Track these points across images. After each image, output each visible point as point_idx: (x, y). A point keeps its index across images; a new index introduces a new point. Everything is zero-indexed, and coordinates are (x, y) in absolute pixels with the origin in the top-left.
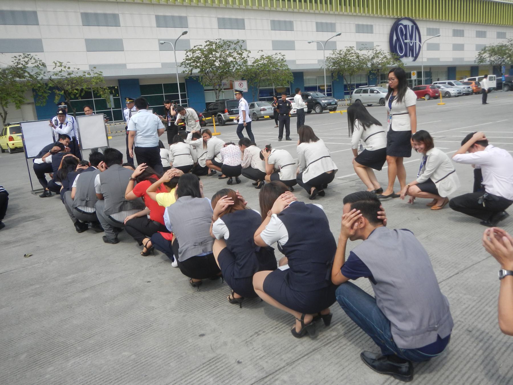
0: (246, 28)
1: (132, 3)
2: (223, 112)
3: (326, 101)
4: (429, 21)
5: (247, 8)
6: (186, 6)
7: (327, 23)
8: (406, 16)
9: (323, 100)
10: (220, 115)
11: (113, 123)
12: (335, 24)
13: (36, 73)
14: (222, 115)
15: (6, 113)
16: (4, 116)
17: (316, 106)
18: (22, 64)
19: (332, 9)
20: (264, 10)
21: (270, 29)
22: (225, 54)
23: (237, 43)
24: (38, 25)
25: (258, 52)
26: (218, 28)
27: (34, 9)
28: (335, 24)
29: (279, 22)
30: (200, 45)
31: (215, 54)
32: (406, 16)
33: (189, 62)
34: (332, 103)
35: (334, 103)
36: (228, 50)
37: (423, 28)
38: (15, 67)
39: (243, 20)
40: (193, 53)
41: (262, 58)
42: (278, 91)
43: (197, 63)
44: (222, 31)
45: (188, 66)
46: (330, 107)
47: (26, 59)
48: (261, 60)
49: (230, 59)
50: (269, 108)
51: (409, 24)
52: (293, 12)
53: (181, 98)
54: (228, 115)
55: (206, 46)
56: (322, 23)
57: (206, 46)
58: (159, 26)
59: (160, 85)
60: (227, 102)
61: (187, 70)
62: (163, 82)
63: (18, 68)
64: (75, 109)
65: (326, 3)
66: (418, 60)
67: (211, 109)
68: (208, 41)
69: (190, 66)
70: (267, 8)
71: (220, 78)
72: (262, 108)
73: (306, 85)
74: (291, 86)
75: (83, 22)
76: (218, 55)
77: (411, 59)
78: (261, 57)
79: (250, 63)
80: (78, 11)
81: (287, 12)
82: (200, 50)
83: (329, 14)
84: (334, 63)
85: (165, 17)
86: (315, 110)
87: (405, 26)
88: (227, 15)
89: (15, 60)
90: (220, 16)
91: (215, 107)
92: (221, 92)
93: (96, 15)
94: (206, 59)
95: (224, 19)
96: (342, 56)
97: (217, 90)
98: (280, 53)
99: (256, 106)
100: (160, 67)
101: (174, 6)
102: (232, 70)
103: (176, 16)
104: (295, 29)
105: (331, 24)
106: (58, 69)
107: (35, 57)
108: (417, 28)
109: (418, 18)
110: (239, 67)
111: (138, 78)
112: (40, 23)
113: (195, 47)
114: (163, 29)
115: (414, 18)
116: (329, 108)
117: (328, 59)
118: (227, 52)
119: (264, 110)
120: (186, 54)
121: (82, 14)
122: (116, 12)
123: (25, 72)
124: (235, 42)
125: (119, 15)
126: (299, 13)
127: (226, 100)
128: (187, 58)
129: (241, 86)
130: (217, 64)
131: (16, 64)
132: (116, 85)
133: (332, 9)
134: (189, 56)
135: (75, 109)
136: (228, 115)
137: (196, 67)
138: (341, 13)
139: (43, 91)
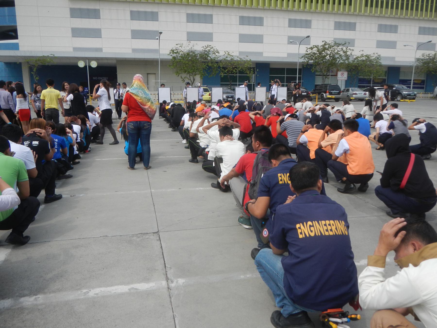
0: (357, 29)
2: (325, 93)
3: (406, 93)
5: (360, 14)
6: (312, 12)
9: (405, 91)
10: (323, 95)
11: (252, 92)
14: (324, 94)
15: (194, 80)
16: (192, 82)
17: (398, 96)
18: (207, 51)
20: (374, 16)
21: (377, 30)
23: (344, 44)
26: (334, 29)
29: (386, 25)
30: (317, 45)
31: (327, 52)
33: (308, 56)
34: (411, 95)
35: (413, 95)
36: (337, 49)
39: (355, 24)
41: (362, 56)
42: (376, 81)
44: (337, 31)
45: (306, 59)
46: (409, 97)
47: (209, 48)
48: (361, 57)
49: (337, 56)
50: (359, 93)
52: (399, 18)
53: (298, 80)
54: (328, 95)
56: (424, 28)
58: (290, 26)
59: (284, 69)
60: (329, 86)
61: (306, 60)
62: (286, 67)
63: (205, 54)
64: (231, 81)
67: (317, 90)
69: (308, 59)
71: (328, 68)
72: (354, 92)
73: (402, 78)
74: (388, 78)
75: (240, 22)
76: (329, 52)
79: (351, 59)
80: (238, 15)
81: (394, 18)
84: (425, 63)
85: (295, 20)
86: (397, 98)
88: (343, 19)
89: (204, 49)
90: (337, 20)
91: (320, 89)
92: (327, 78)
93: (249, 18)
94: (320, 55)
95: (339, 23)
96: (431, 58)
97: (324, 75)
98: (377, 53)
99: (350, 90)
100: (286, 55)
101: (303, 12)
102: (337, 63)
104: (399, 32)
107: (214, 48)
110: (342, 62)
112: (214, 22)
114: (293, 29)
116: (408, 98)
117: (418, 60)
118: (336, 51)
119: (356, 94)
120: (306, 50)
121: (240, 17)
122: (262, 16)
123: (208, 56)
124: (343, 44)
125: (263, 18)
126: (404, 18)
127: (329, 84)
128: (307, 53)
129: (343, 76)
131: (204, 51)
134: (308, 51)
135: (231, 81)
136: (328, 95)
137: (312, 59)
139: (216, 69)
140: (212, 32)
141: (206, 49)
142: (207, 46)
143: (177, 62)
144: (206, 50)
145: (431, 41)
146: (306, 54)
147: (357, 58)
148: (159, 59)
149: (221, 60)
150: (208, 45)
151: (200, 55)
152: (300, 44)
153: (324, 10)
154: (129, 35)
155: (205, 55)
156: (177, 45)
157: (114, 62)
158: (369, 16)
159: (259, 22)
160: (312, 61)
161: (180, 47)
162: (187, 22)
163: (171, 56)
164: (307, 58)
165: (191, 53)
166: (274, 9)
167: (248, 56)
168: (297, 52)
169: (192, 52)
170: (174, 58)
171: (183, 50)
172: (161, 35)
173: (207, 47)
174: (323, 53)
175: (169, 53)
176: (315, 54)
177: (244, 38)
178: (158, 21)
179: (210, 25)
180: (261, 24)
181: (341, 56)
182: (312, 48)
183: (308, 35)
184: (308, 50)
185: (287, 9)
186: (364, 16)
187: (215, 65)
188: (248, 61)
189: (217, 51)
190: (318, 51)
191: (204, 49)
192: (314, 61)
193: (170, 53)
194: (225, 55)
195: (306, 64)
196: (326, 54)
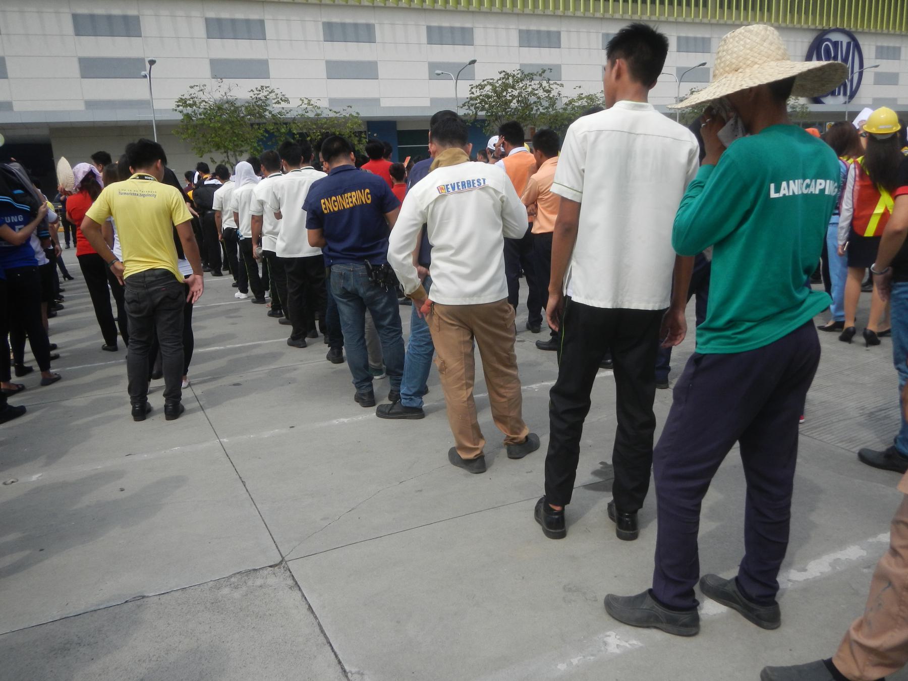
0: (562, 46)
1: (394, 8)
4: (882, 34)
6: (473, 12)
7: (695, 39)
8: (838, 26)
12: (709, 39)
13: (278, 113)
18: (261, 100)
19: (705, 15)
20: (594, 18)
22: (526, 92)
24: (265, 39)
25: (575, 88)
26: (518, 45)
27: (262, 18)
28: (709, 39)
30: (491, 79)
32: (838, 26)
36: (530, 85)
37: (868, 47)
38: (254, 104)
39: (559, 33)
40: (480, 89)
41: (580, 98)
43: (485, 104)
45: (472, 108)
47: (266, 94)
49: (533, 99)
51: (844, 39)
55: (500, 80)
56: (687, 38)
57: (500, 80)
58: (430, 41)
63: (258, 106)
65: (697, 5)
66: (855, 100)
68: (504, 71)
70: (598, 15)
76: (516, 93)
77: (841, 99)
78: (579, 96)
79: (560, 105)
80: (320, 20)
82: (491, 84)
83: (701, 24)
85: (440, 28)
87: (835, 44)
89: (254, 95)
90: (524, 27)
93: (343, 25)
95: (528, 32)
101: (455, 12)
102: (535, 114)
103: (458, 28)
105: (703, 39)
106: (304, 106)
107: (277, 91)
108: (857, 47)
109: (860, 29)
110: (543, 111)
111: (395, 120)
112: (267, 38)
113: (484, 81)
115: (853, 29)
118: (530, 90)
120: (470, 91)
121: (324, 23)
122: (372, 21)
123: (265, 110)
130: (514, 104)
131: (255, 100)
132: (363, 128)
133: (705, 15)
134: (475, 93)
137: (483, 109)
138: (722, 22)
140: (265, 57)
141: (258, 94)
142: (259, 88)
143: (196, 126)
144: (259, 98)
145: (704, 64)
146: (471, 99)
147: (570, 102)
148: (152, 121)
149: (295, 118)
150: (262, 86)
151: (246, 108)
152: (457, 80)
153: (497, 6)
154: (75, 69)
155: (257, 107)
156: (192, 87)
157: (45, 132)
158: (584, 18)
159: (366, 34)
160: (483, 113)
161: (199, 91)
162: (208, 38)
163: (181, 112)
164: (473, 107)
165: (227, 105)
166: (395, 6)
167: (351, 107)
168: (454, 96)
169: (227, 102)
170: (188, 116)
171: (206, 100)
172: (152, 66)
173: (260, 91)
174: (505, 94)
175: (174, 107)
176: (488, 97)
177: (336, 70)
178: (141, 37)
179: (261, 43)
180: (371, 39)
181: (539, 98)
182: (481, 87)
183: (473, 59)
184: (474, 90)
185: (422, 6)
186: (574, 17)
187: (283, 127)
188: (353, 116)
189: (283, 98)
190: (494, 90)
191: (254, 95)
192: (487, 112)
193: (178, 106)
194: (301, 105)
195: (473, 117)
196: (510, 96)
